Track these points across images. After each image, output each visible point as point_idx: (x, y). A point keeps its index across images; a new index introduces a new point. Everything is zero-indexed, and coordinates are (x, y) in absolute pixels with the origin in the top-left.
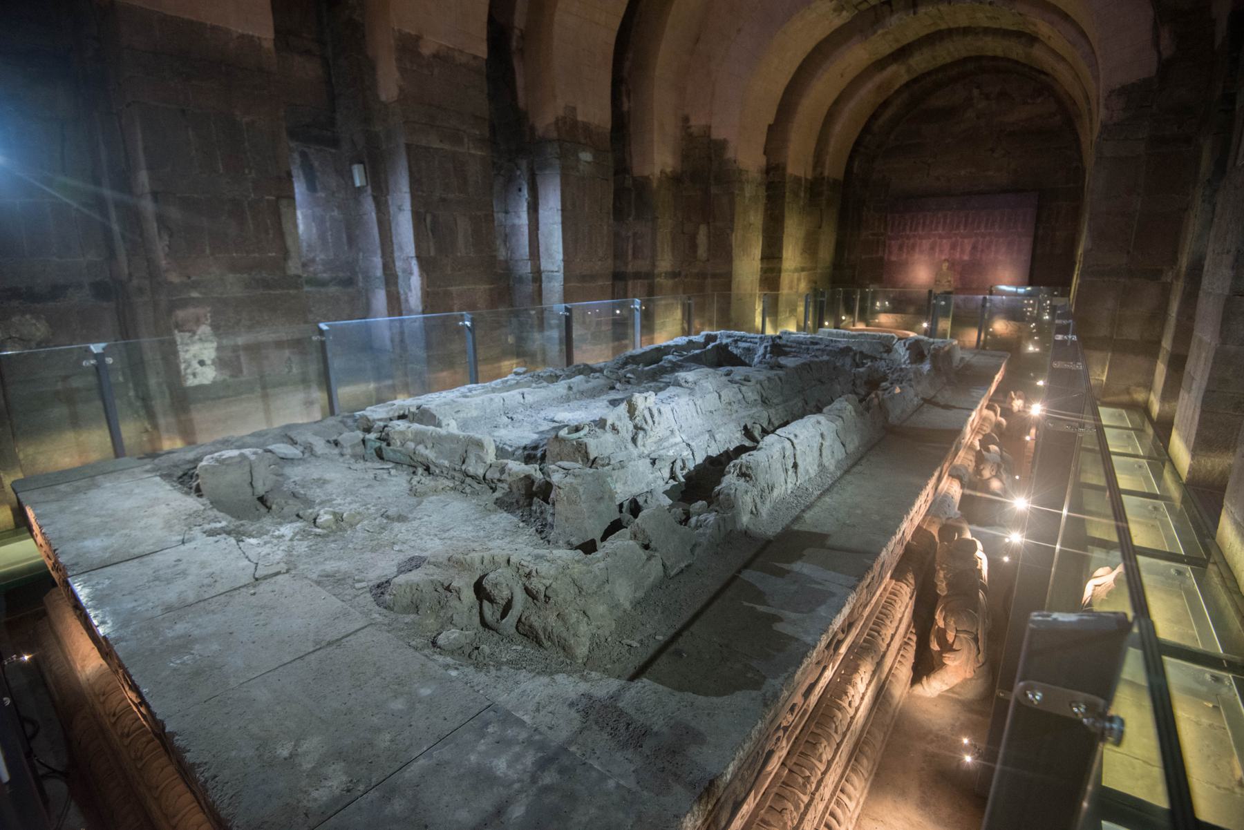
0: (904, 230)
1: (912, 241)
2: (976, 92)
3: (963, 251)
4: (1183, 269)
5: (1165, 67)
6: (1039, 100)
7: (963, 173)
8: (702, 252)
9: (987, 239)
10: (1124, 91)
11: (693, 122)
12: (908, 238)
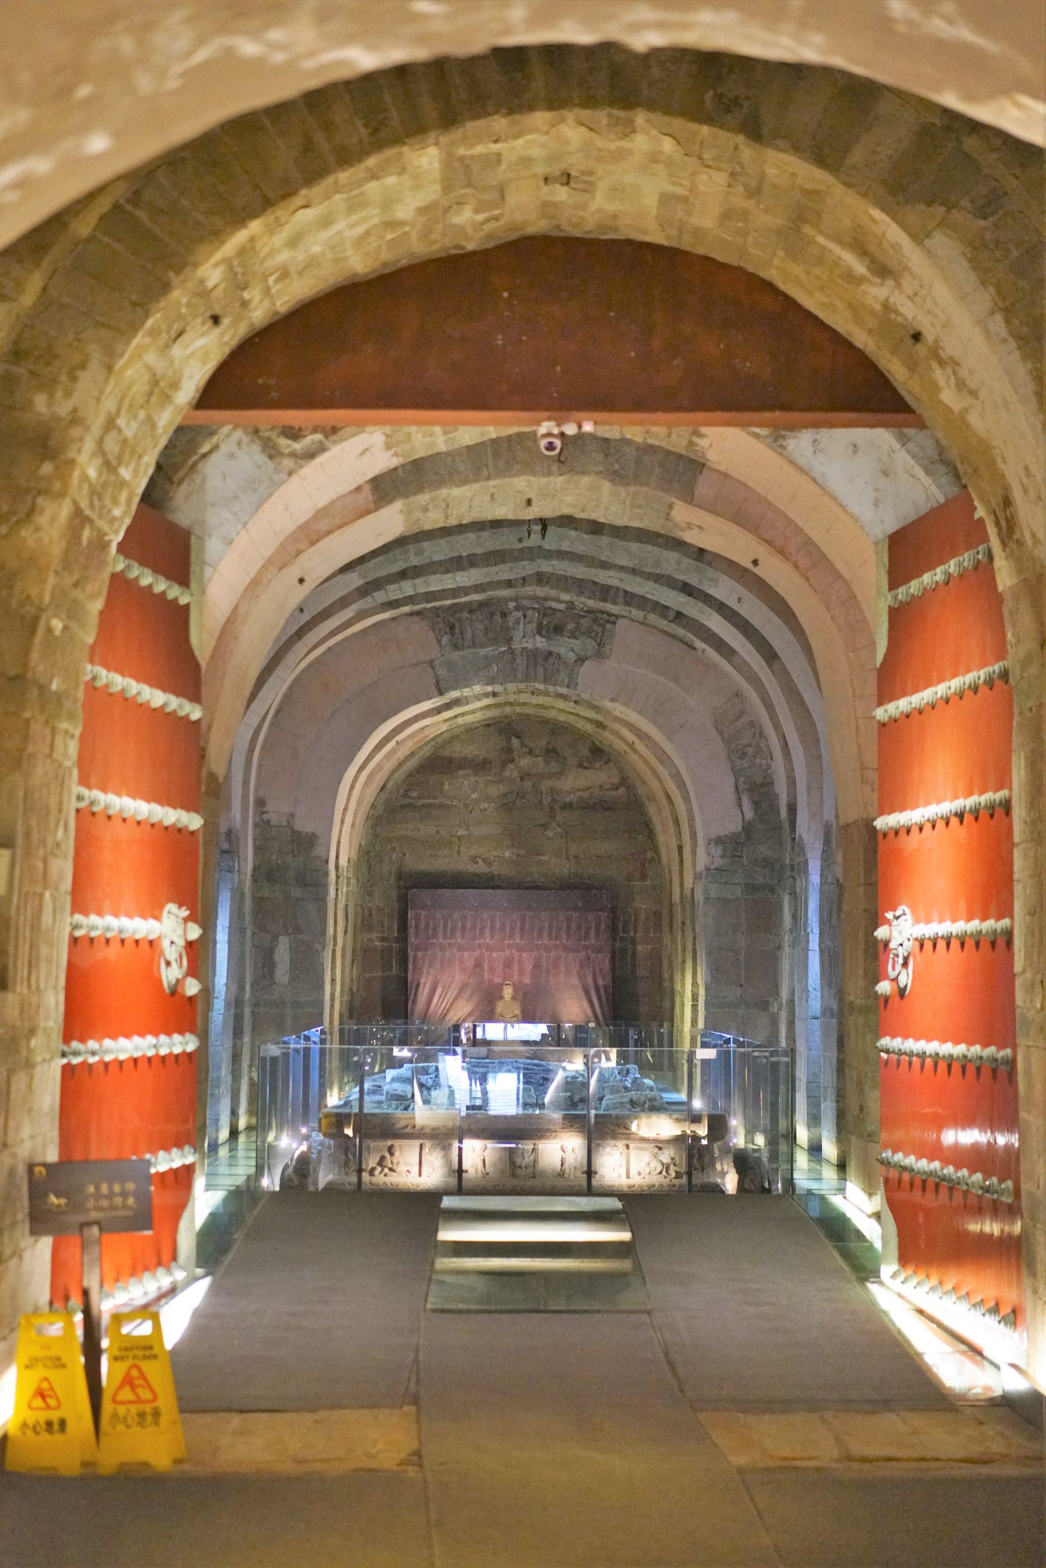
0: (435, 936)
1: (448, 953)
2: (515, 742)
3: (492, 970)
4: (784, 1001)
5: (748, 828)
6: (597, 765)
7: (507, 854)
8: (282, 973)
9: (553, 954)
10: (719, 841)
11: (269, 807)
12: (442, 948)
